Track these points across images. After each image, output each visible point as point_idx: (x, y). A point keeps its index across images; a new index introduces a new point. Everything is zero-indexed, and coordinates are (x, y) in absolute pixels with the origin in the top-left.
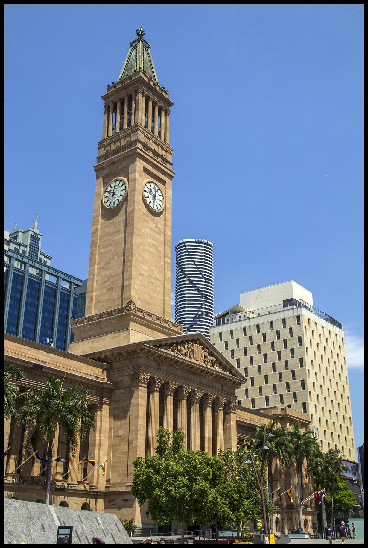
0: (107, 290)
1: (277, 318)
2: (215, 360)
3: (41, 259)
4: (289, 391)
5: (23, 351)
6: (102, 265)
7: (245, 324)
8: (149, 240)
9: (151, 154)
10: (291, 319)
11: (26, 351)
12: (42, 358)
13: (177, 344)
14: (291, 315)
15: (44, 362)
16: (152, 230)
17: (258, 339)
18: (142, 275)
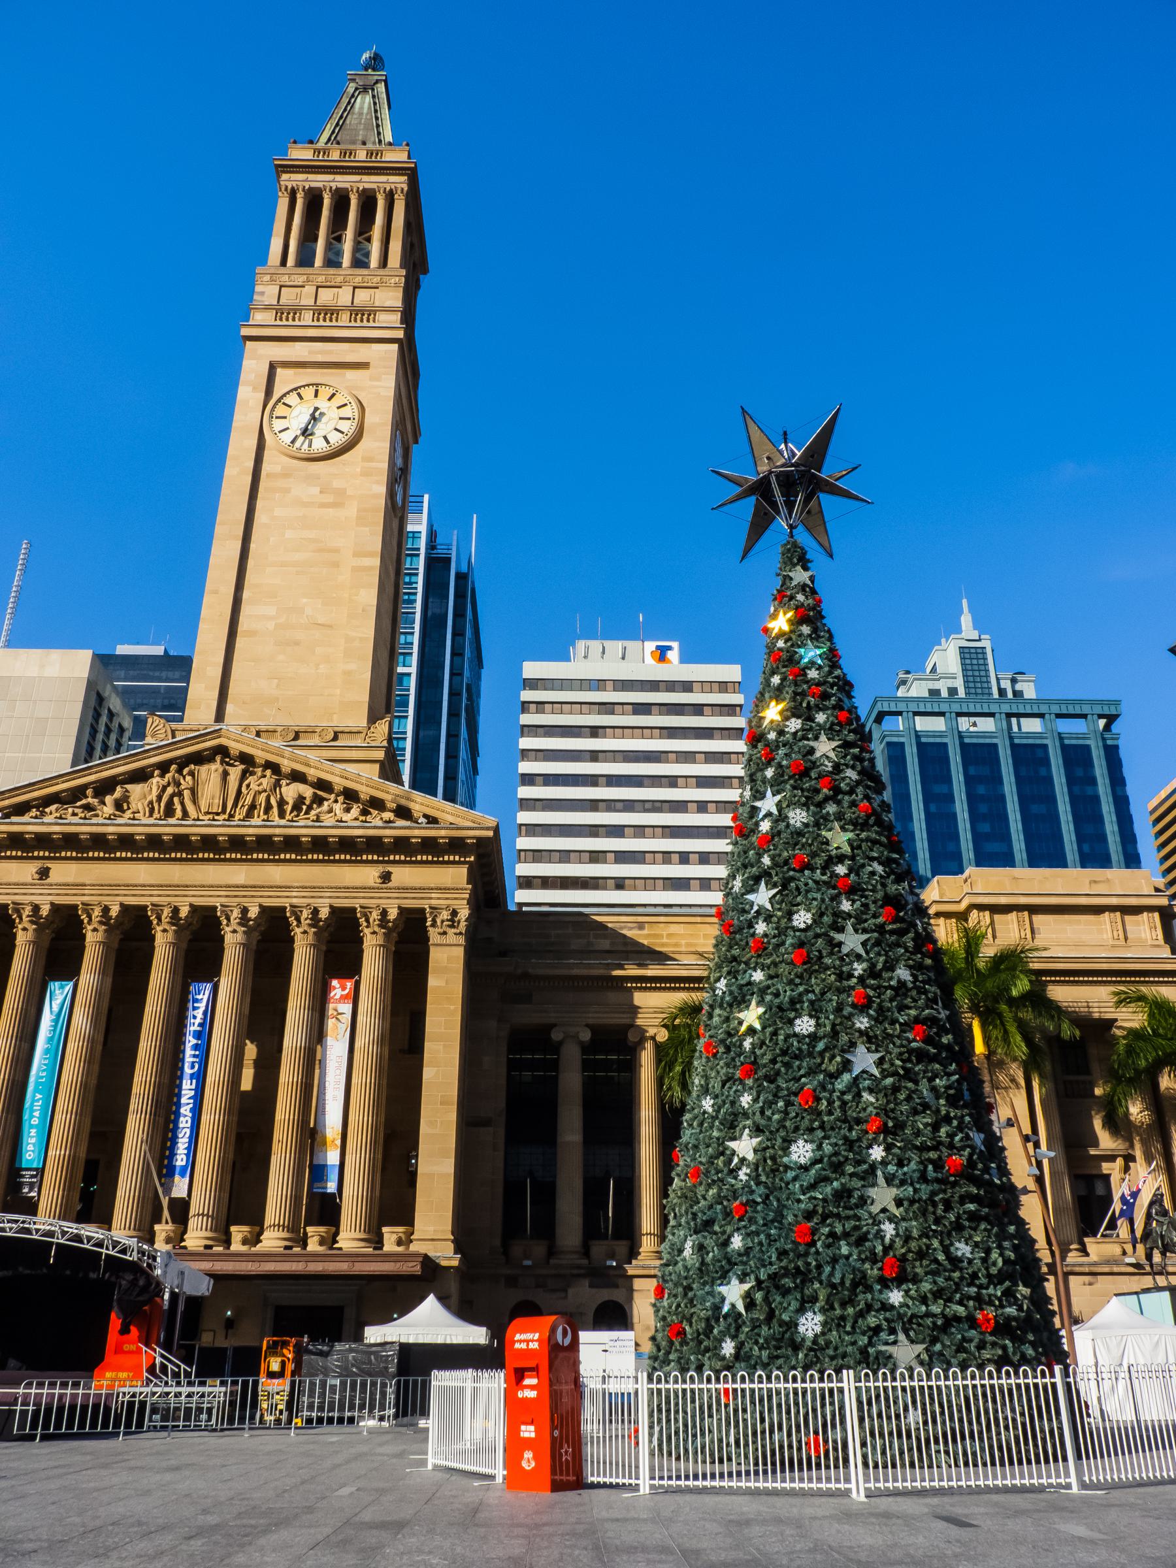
2: (308, 792)
3: (1002, 692)
18: (252, 633)
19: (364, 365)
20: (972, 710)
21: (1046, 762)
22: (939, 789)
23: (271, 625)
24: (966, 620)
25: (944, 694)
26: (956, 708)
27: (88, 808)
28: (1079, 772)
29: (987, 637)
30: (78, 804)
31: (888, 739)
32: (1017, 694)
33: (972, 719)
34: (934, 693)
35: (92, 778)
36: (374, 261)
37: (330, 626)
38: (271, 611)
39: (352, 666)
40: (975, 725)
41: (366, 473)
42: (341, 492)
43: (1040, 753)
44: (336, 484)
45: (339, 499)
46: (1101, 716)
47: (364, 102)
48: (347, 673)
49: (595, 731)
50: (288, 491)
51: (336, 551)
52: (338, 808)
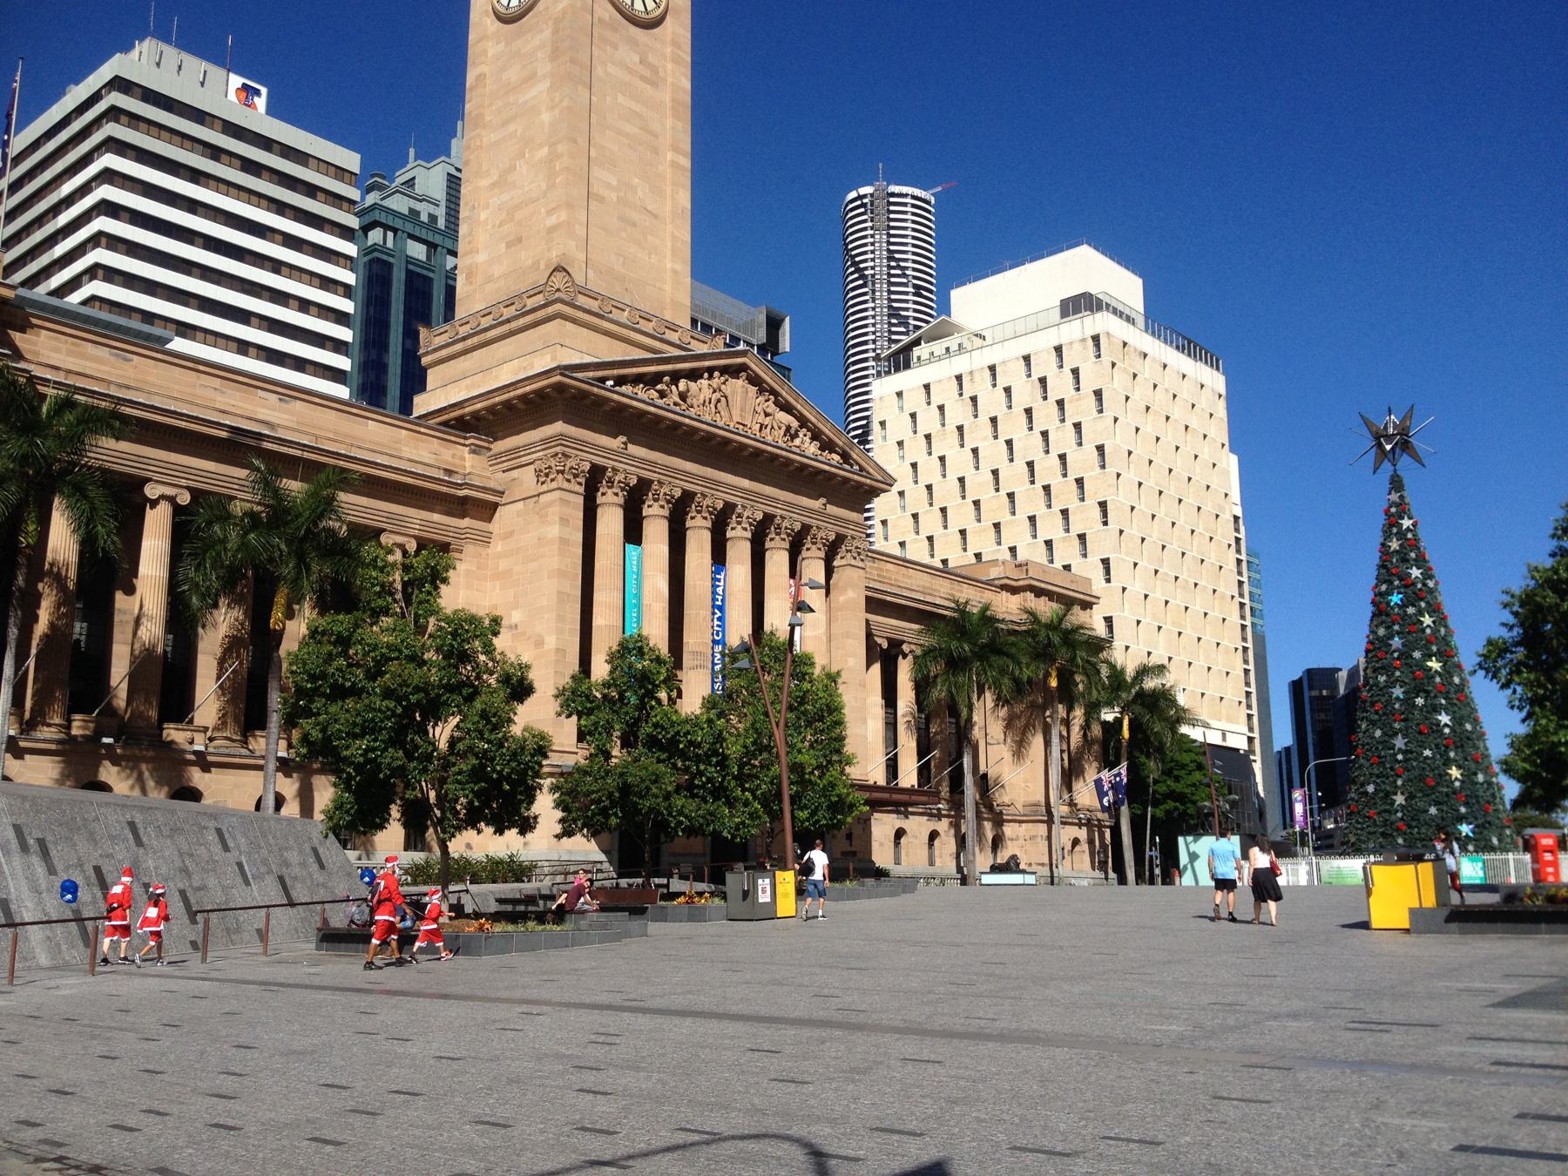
0: (509, 245)
1: (1040, 346)
2: (795, 424)
4: (1067, 531)
5: (199, 391)
6: (495, 178)
7: (960, 364)
8: (621, 99)
10: (1077, 346)
11: (209, 393)
12: (263, 413)
13: (676, 377)
14: (1079, 336)
16: (630, 71)
17: (992, 402)
18: (601, 199)
23: (614, 196)
25: (424, 218)
30: (659, 387)
31: (376, 254)
34: (414, 213)
35: (669, 367)
37: (656, 216)
39: (678, 267)
42: (654, 69)
48: (674, 272)
49: (196, 176)
50: (615, 47)
51: (656, 136)
52: (807, 439)
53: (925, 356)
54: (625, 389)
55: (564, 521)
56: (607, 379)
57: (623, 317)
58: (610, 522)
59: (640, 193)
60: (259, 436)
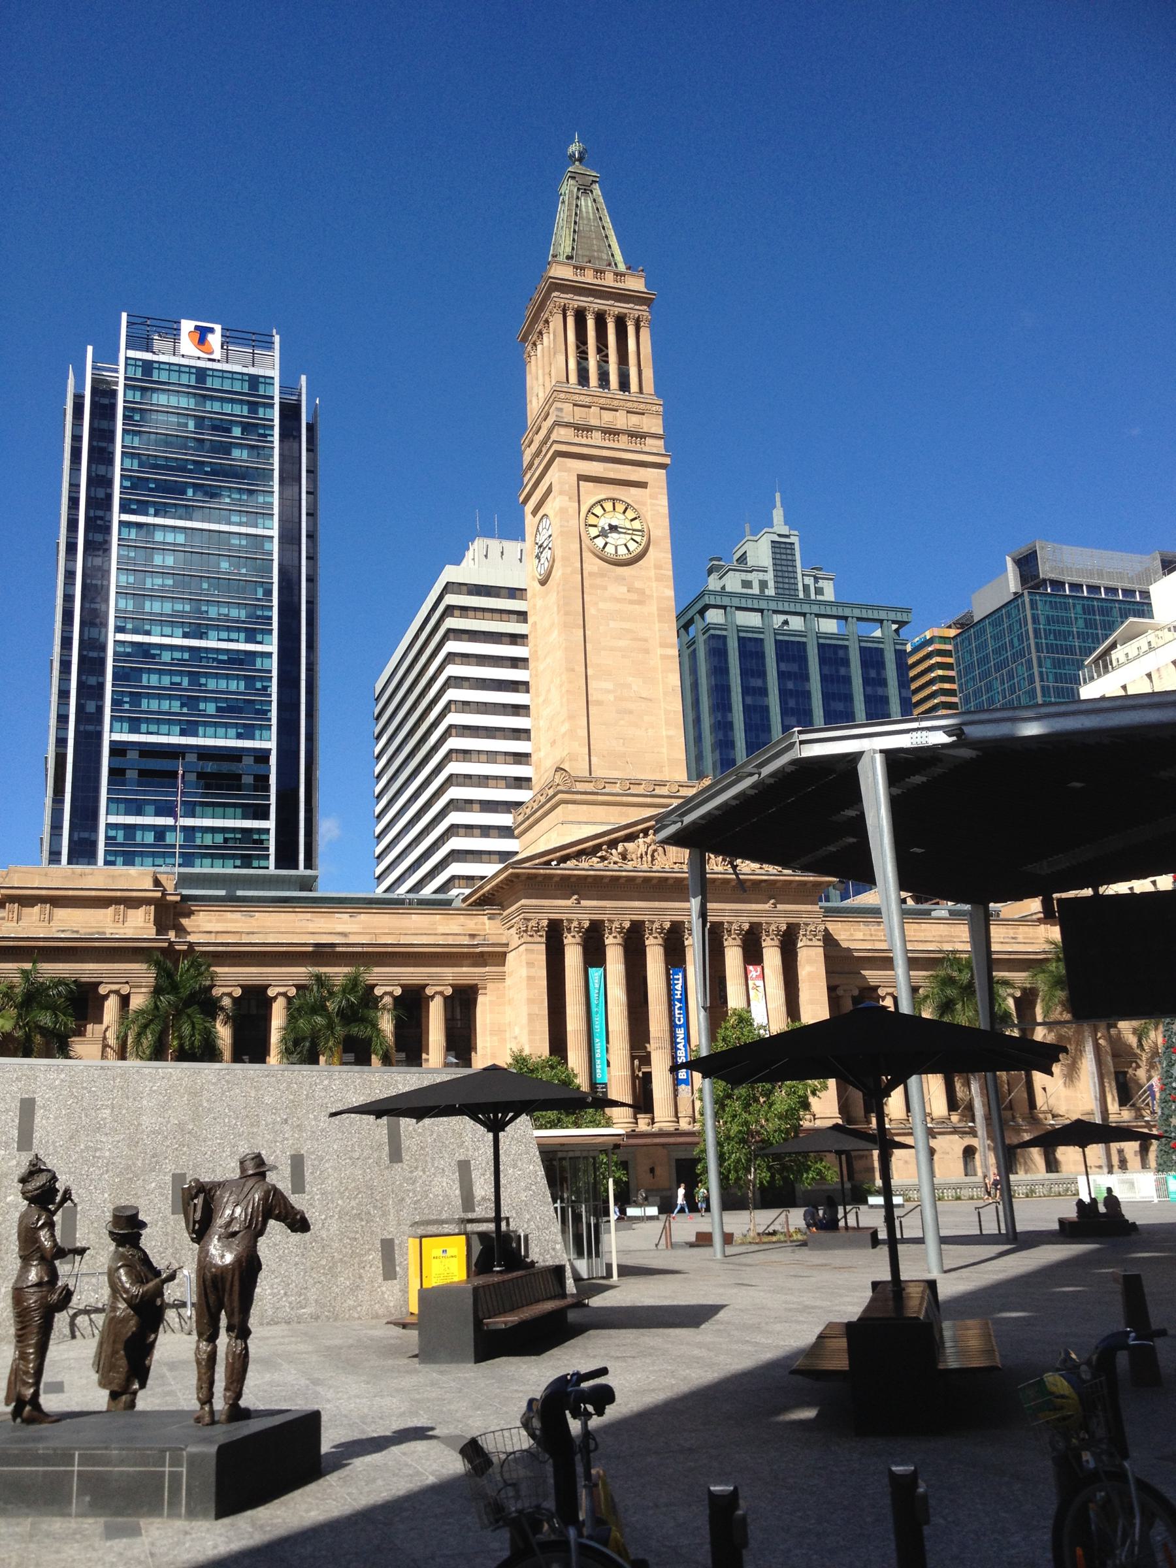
3: (806, 588)
9: (597, 438)
11: (304, 923)
12: (340, 928)
13: (613, 844)
15: (344, 934)
16: (618, 600)
18: (599, 703)
19: (642, 485)
20: (787, 609)
21: (846, 662)
22: (756, 683)
23: (611, 697)
24: (778, 515)
26: (773, 605)
27: (603, 859)
28: (873, 674)
29: (796, 533)
30: (599, 854)
31: (712, 632)
32: (819, 591)
33: (782, 618)
34: (747, 584)
35: (606, 839)
36: (634, 386)
38: (609, 685)
39: (672, 733)
40: (786, 622)
41: (659, 579)
42: (641, 592)
43: (841, 653)
44: (638, 584)
45: (641, 598)
46: (894, 622)
47: (586, 204)
48: (669, 737)
50: (605, 588)
51: (646, 640)
53: (1122, 659)
54: (570, 864)
55: (530, 964)
56: (552, 860)
57: (617, 789)
58: (573, 956)
59: (635, 687)
60: (333, 945)
